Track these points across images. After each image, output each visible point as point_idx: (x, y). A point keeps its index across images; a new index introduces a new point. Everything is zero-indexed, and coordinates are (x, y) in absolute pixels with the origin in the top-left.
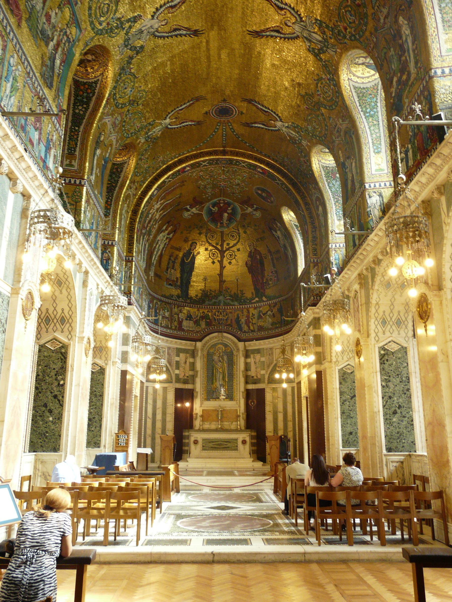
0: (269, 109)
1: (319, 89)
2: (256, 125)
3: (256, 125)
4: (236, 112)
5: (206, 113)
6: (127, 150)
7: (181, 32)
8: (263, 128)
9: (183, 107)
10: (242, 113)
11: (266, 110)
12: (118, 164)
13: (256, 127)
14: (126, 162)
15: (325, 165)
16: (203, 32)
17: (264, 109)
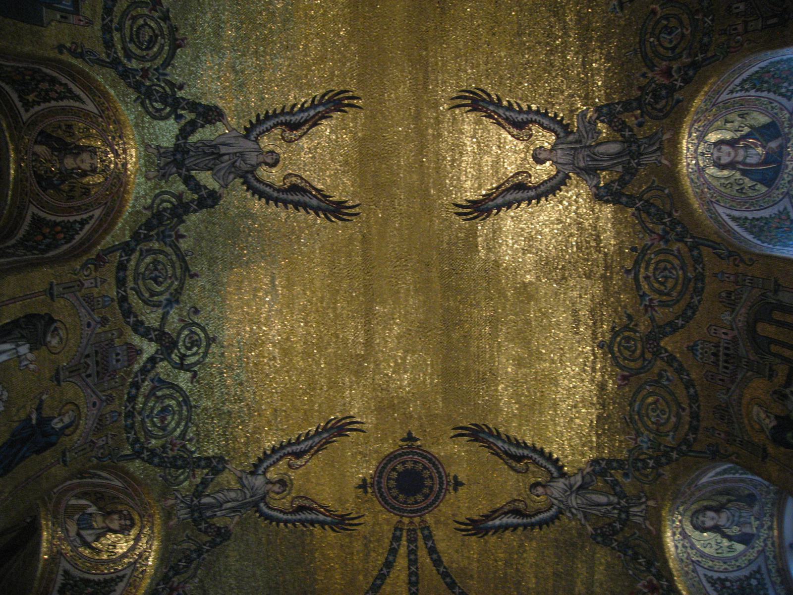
0: (526, 446)
1: (645, 287)
2: (497, 522)
3: (497, 522)
4: (441, 483)
5: (363, 485)
6: (133, 532)
7: (306, 199)
8: (515, 527)
9: (303, 446)
10: (458, 484)
11: (520, 452)
12: (98, 583)
13: (497, 529)
14: (121, 578)
15: (716, 575)
16: (357, 210)
17: (513, 450)
